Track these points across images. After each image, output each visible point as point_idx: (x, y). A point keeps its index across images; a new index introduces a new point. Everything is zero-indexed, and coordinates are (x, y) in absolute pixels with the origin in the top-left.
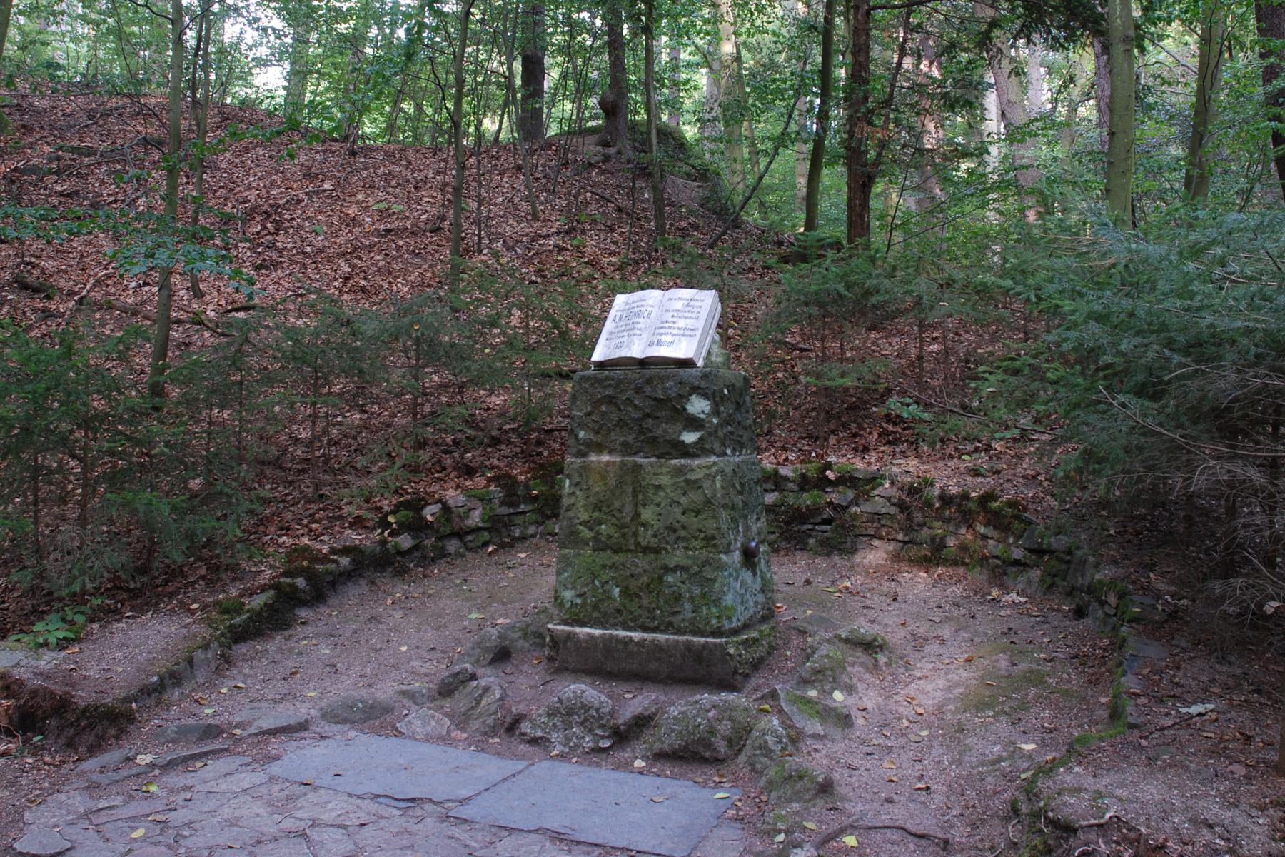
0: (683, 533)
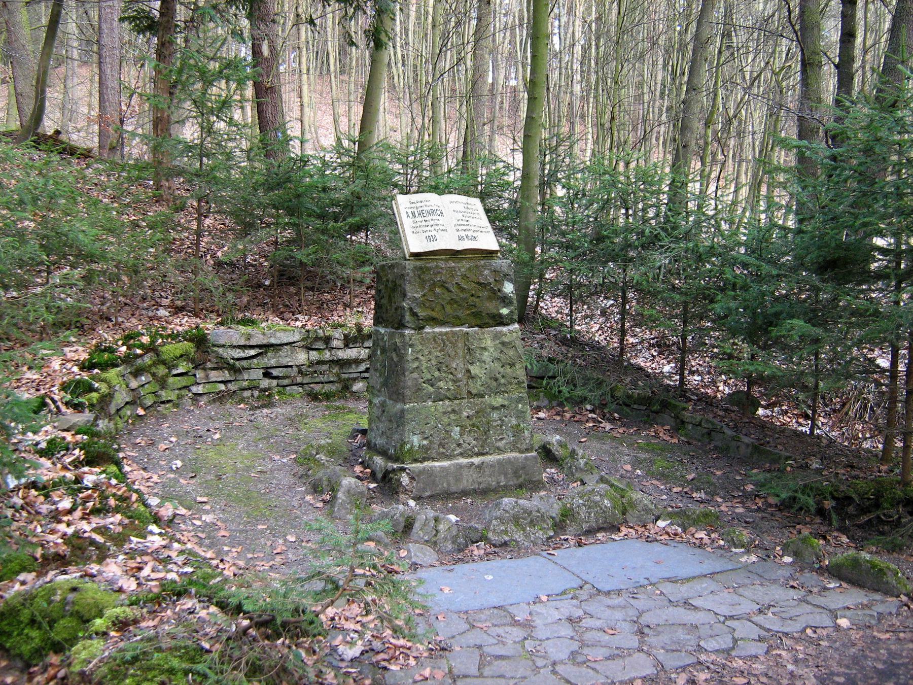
0: (503, 381)
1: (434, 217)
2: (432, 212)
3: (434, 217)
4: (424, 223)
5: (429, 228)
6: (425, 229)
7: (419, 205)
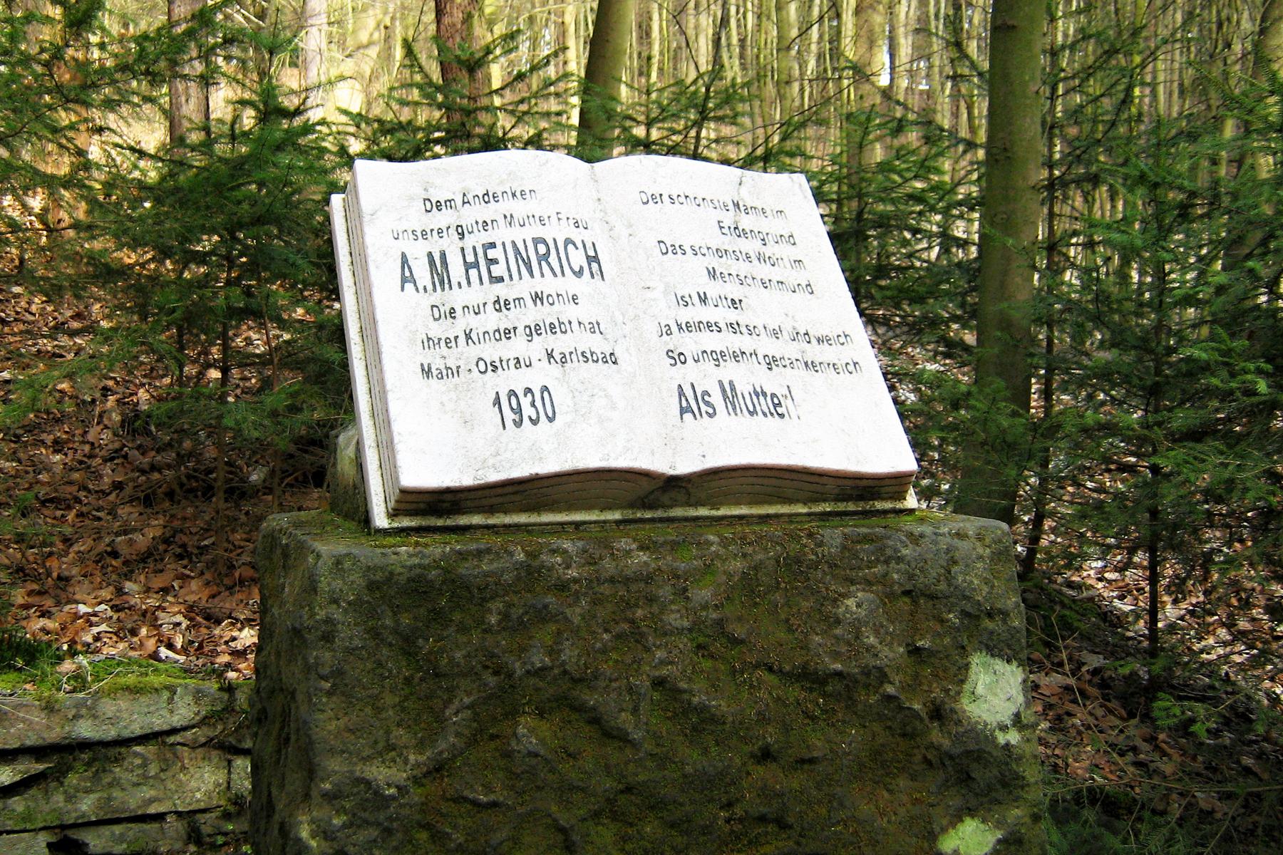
1: (548, 284)
2: (538, 256)
3: (548, 284)
4: (491, 320)
5: (518, 347)
6: (491, 351)
7: (468, 215)
